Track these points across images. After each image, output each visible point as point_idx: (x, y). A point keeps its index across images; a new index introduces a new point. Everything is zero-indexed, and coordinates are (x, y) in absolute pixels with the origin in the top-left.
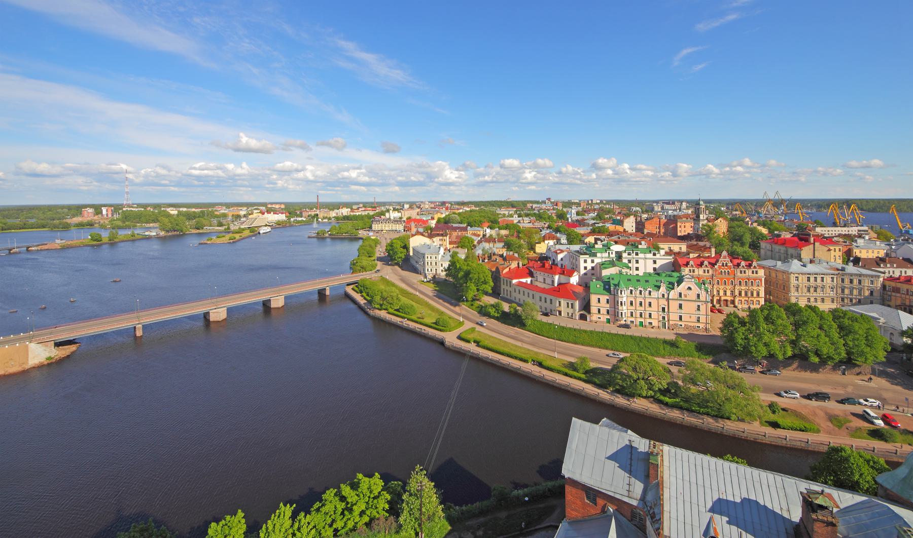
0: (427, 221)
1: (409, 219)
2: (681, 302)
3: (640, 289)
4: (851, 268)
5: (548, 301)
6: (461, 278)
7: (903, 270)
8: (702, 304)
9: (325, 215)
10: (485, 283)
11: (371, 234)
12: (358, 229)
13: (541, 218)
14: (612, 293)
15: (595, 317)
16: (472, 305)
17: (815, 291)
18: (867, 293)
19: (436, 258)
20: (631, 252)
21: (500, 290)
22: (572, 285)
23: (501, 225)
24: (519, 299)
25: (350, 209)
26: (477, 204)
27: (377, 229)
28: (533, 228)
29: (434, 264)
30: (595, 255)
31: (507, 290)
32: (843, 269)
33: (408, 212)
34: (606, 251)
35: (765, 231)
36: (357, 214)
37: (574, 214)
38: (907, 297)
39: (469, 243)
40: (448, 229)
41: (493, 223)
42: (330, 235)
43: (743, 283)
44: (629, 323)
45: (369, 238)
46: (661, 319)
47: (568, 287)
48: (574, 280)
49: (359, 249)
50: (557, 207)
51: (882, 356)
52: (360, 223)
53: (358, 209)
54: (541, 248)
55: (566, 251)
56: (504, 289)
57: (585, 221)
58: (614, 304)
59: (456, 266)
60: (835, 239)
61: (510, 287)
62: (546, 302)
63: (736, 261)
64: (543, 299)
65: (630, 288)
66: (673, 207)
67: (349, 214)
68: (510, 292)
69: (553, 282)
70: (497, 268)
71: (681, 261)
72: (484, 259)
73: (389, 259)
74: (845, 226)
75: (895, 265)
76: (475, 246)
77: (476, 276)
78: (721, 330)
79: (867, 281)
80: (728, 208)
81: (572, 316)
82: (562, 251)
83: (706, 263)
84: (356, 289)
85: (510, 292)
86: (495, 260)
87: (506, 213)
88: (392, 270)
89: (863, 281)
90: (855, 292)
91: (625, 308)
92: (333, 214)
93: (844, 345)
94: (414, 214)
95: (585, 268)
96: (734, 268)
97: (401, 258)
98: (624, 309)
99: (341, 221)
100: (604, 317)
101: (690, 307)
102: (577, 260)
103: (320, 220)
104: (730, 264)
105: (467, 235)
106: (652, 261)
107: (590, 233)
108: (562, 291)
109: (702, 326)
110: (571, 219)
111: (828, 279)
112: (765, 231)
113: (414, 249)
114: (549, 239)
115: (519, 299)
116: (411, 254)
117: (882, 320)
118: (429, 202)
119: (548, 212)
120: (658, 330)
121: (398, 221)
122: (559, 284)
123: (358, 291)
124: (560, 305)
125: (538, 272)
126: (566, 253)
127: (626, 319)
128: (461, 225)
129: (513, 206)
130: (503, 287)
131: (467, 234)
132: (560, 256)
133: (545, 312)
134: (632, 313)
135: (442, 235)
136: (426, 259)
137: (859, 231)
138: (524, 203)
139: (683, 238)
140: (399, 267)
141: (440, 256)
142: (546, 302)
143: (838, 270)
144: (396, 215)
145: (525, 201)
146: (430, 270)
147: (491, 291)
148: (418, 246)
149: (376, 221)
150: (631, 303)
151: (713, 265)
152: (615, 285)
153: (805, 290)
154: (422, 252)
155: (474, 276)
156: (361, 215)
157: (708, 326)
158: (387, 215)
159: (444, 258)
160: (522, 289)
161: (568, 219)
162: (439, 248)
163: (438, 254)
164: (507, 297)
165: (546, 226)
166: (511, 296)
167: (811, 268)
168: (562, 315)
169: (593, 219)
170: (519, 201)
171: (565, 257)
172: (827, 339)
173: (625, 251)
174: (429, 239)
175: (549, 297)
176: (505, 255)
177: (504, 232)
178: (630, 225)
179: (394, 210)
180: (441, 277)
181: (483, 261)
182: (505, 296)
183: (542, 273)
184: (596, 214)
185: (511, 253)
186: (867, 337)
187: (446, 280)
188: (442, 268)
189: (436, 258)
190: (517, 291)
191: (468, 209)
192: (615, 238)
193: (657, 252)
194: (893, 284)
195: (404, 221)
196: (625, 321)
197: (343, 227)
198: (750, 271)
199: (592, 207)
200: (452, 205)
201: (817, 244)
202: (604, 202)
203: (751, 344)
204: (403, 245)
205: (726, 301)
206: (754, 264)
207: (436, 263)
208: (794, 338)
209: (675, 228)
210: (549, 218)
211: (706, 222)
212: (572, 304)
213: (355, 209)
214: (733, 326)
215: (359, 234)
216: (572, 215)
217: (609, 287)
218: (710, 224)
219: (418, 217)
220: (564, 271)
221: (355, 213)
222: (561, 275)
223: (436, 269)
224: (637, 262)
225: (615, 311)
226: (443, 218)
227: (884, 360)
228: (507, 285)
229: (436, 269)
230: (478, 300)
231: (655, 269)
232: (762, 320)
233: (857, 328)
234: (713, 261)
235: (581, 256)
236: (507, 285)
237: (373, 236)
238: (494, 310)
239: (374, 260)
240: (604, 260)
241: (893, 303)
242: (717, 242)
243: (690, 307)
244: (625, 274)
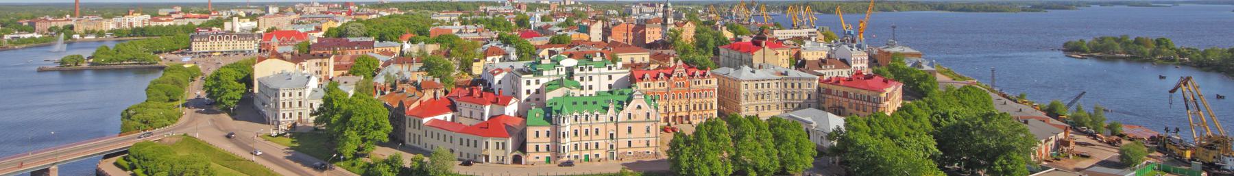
0: (305, 34)
1: (271, 32)
2: (630, 125)
3: (586, 113)
4: (794, 73)
5: (472, 143)
6: (337, 124)
7: (840, 71)
8: (652, 125)
9: (91, 28)
10: (377, 127)
11: (187, 59)
12: (160, 52)
13: (494, 25)
14: (554, 122)
15: (531, 157)
16: (354, 165)
17: (763, 98)
18: (806, 97)
19: (300, 94)
20: (584, 67)
21: (404, 136)
22: (508, 117)
23: (432, 36)
24: (432, 146)
25: (149, 17)
27: (201, 50)
28: (479, 39)
30: (540, 73)
32: (786, 74)
33: (272, 19)
34: (554, 67)
35: (729, 35)
36: (165, 24)
37: (538, 19)
38: (837, 98)
39: (368, 66)
40: (339, 45)
41: (421, 33)
42: (92, 64)
43: (698, 95)
44: (572, 158)
45: (180, 67)
46: (609, 148)
47: (502, 121)
48: (511, 109)
49: (148, 88)
50: (519, 10)
51: (810, 161)
52: (166, 41)
53: (170, 15)
54: (477, 69)
55: (507, 70)
56: (410, 134)
57: (549, 29)
58: (556, 136)
59: (333, 105)
60: (787, 41)
61: (419, 129)
62: (468, 145)
63: (691, 71)
64: (465, 142)
65: (575, 114)
66: (651, 9)
67: (147, 25)
68: (419, 136)
69: (482, 115)
70: (401, 103)
71: (637, 74)
72: (385, 90)
73: (211, 104)
74: (798, 28)
75: (833, 66)
76: (378, 70)
77: (361, 119)
78: (668, 152)
79: (805, 84)
80: (705, 11)
81: (503, 160)
82: (501, 71)
83: (662, 75)
84: (124, 163)
85: (419, 136)
86: (401, 90)
87: (447, 19)
88: (213, 120)
89: (802, 85)
90: (796, 96)
91: (567, 140)
92: (110, 25)
93: (778, 154)
94: (284, 23)
95: (528, 92)
96: (689, 78)
97: (234, 99)
98: (567, 142)
99: (128, 38)
100: (543, 156)
101: (639, 130)
102: (519, 82)
103: (77, 36)
104: (685, 75)
105: (371, 54)
106: (607, 76)
107: (549, 44)
108: (495, 127)
109: (651, 150)
110: (534, 26)
111: (773, 84)
112: (729, 35)
113: (260, 83)
114: (492, 54)
115: (432, 146)
116: (256, 90)
117: (814, 124)
118: (320, 3)
119: (506, 18)
120: (605, 162)
121: (243, 36)
122: (491, 117)
123: (127, 167)
124: (487, 147)
125: (463, 104)
126: (506, 73)
127: (569, 155)
128: (365, 39)
129: (459, 10)
130: (408, 130)
131: (373, 52)
132: (497, 78)
133: (467, 159)
134: (576, 145)
135: (321, 56)
136: (281, 97)
137: (810, 33)
139: (651, 46)
140: (230, 114)
141: (308, 92)
142: (468, 145)
143: (782, 74)
144: (248, 24)
145: (477, 2)
146: (287, 115)
147: (387, 140)
148: (268, 77)
149: (201, 37)
150: (576, 133)
151: (668, 76)
152: (557, 112)
153: (754, 98)
154: (274, 86)
155: (357, 119)
156: (175, 25)
157: (659, 150)
158: (228, 26)
159: (316, 94)
160: (436, 131)
161: (530, 27)
162: (309, 77)
163: (305, 87)
164: (413, 145)
165: (496, 36)
166: (419, 144)
167: (759, 74)
168: (490, 161)
169: (559, 26)
170: (468, 2)
171: (504, 78)
172: (764, 151)
173: (577, 66)
174: (294, 64)
175: (472, 138)
176: (419, 82)
177: (431, 48)
178: (596, 32)
179: (248, 15)
180: (307, 125)
181: (382, 93)
182: (412, 144)
183: (468, 105)
184: (565, 18)
185: (430, 78)
186: (797, 144)
187: (316, 129)
188: (309, 111)
189: (300, 94)
190: (429, 134)
191: (385, 14)
192: (573, 50)
193: (612, 65)
194: (826, 86)
195: (260, 36)
196: (569, 157)
197: (124, 49)
198: (704, 81)
199: (564, 10)
200: (360, 7)
201: (767, 48)
202: (580, 3)
203: (695, 166)
204: (241, 76)
205: (681, 117)
206: (708, 73)
207: (300, 103)
208: (734, 154)
209: (644, 33)
210: (505, 26)
211: (673, 26)
212: (503, 144)
213: (164, 16)
214: (678, 147)
215: (160, 60)
216: (536, 20)
217: (551, 115)
218: (677, 29)
219: (290, 29)
220: (497, 99)
221: (160, 24)
222: (494, 105)
223: (300, 113)
224: (591, 79)
225: (556, 145)
227: (812, 166)
228: (415, 128)
229: (300, 113)
230: (363, 156)
231: (610, 86)
232: (705, 137)
233: (789, 135)
234: (669, 72)
235: (523, 76)
236: (415, 128)
237: (189, 63)
238: (388, 167)
239: (179, 106)
240: (551, 79)
241: (826, 106)
242: (682, 49)
243: (639, 130)
244: (571, 95)
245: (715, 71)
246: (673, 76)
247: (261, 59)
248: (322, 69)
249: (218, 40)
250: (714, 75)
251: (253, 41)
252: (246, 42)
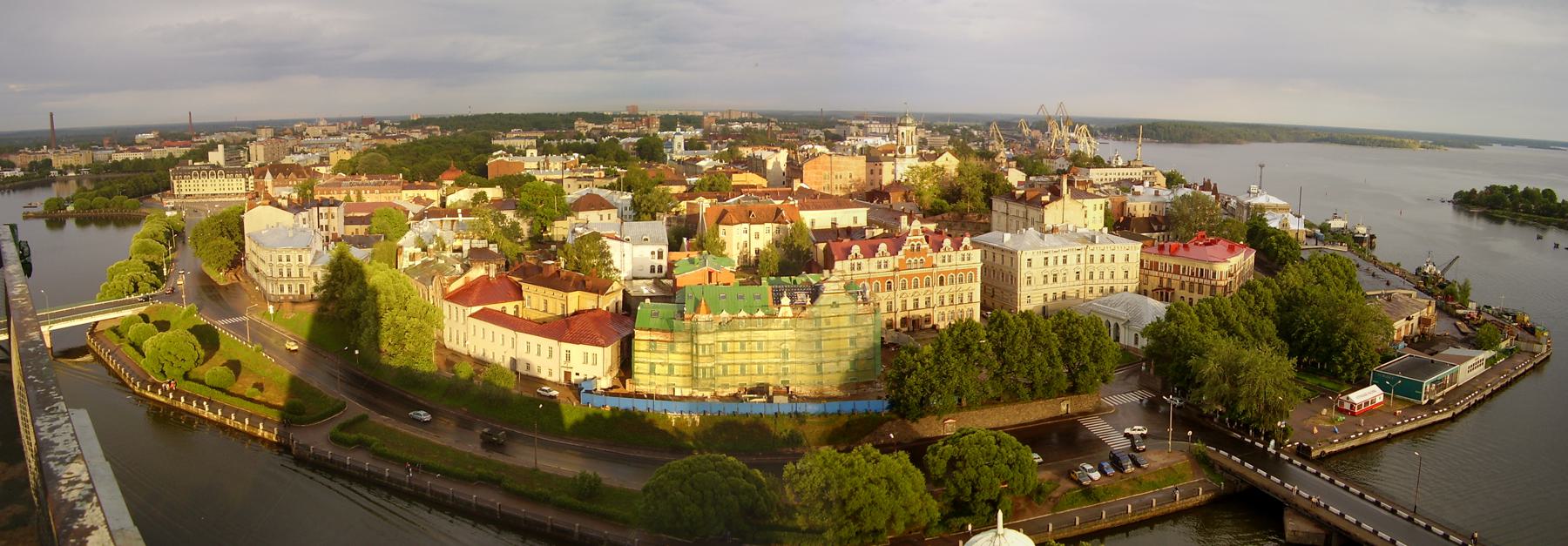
19: (300, 260)
26: (445, 122)
29: (295, 273)
138: (568, 120)
189: (300, 260)
200: (383, 125)
223: (302, 286)
229: (302, 286)
245: (974, 238)
246: (904, 248)
247: (251, 207)
248: (329, 222)
250: (975, 245)
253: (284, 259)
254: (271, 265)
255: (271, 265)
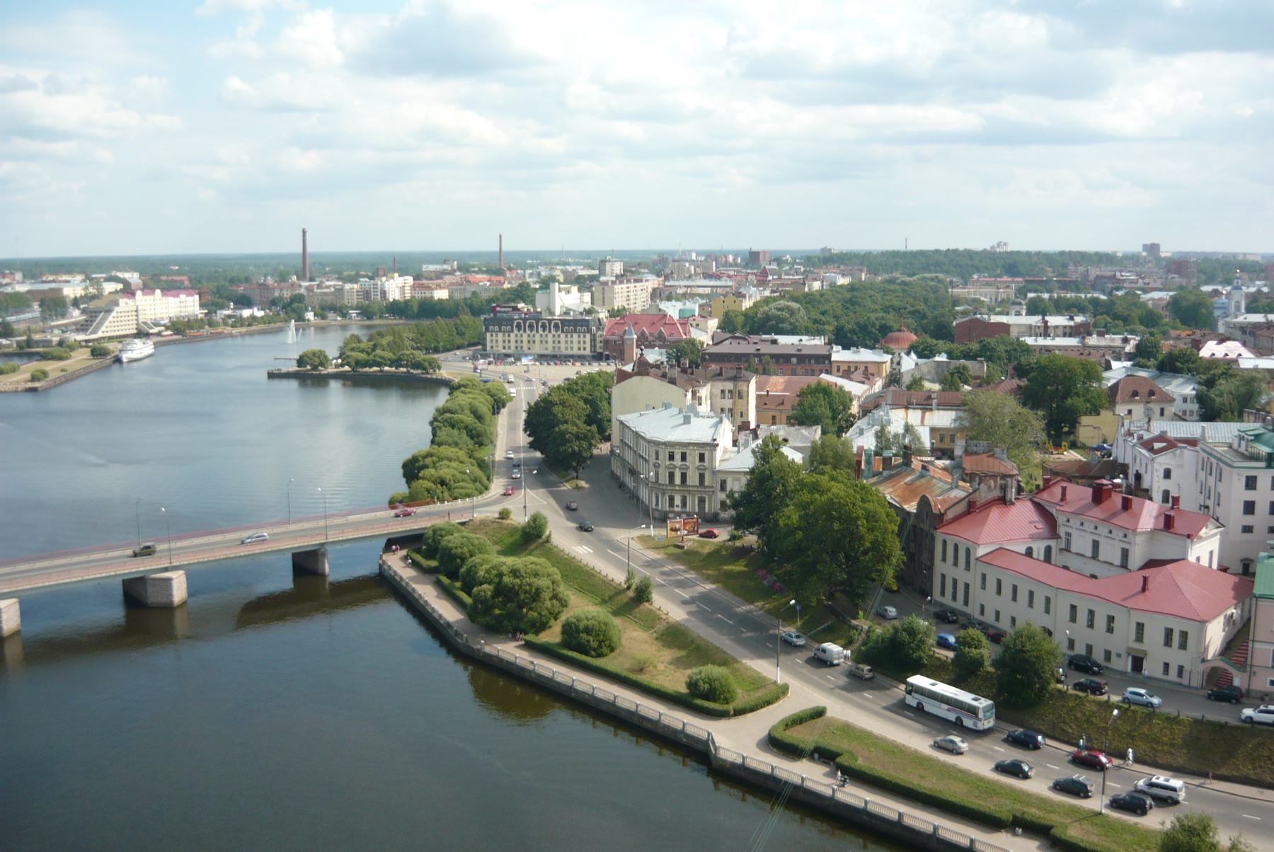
5: (1101, 622)
19: (702, 458)
24: (998, 613)
25: (410, 280)
29: (693, 479)
31: (955, 582)
56: (943, 576)
61: (968, 567)
62: (1091, 625)
64: (1082, 616)
67: (408, 296)
68: (967, 586)
85: (967, 586)
115: (998, 613)
125: (1075, 522)
130: (940, 568)
142: (1091, 625)
164: (952, 604)
166: (966, 603)
182: (947, 600)
189: (702, 458)
207: (702, 477)
223: (702, 501)
226: (745, 314)
228: (956, 564)
229: (702, 501)
236: (956, 564)
249: (540, 329)
251: (588, 336)
252: (575, 335)
253: (678, 457)
254: (657, 466)
255: (657, 466)
